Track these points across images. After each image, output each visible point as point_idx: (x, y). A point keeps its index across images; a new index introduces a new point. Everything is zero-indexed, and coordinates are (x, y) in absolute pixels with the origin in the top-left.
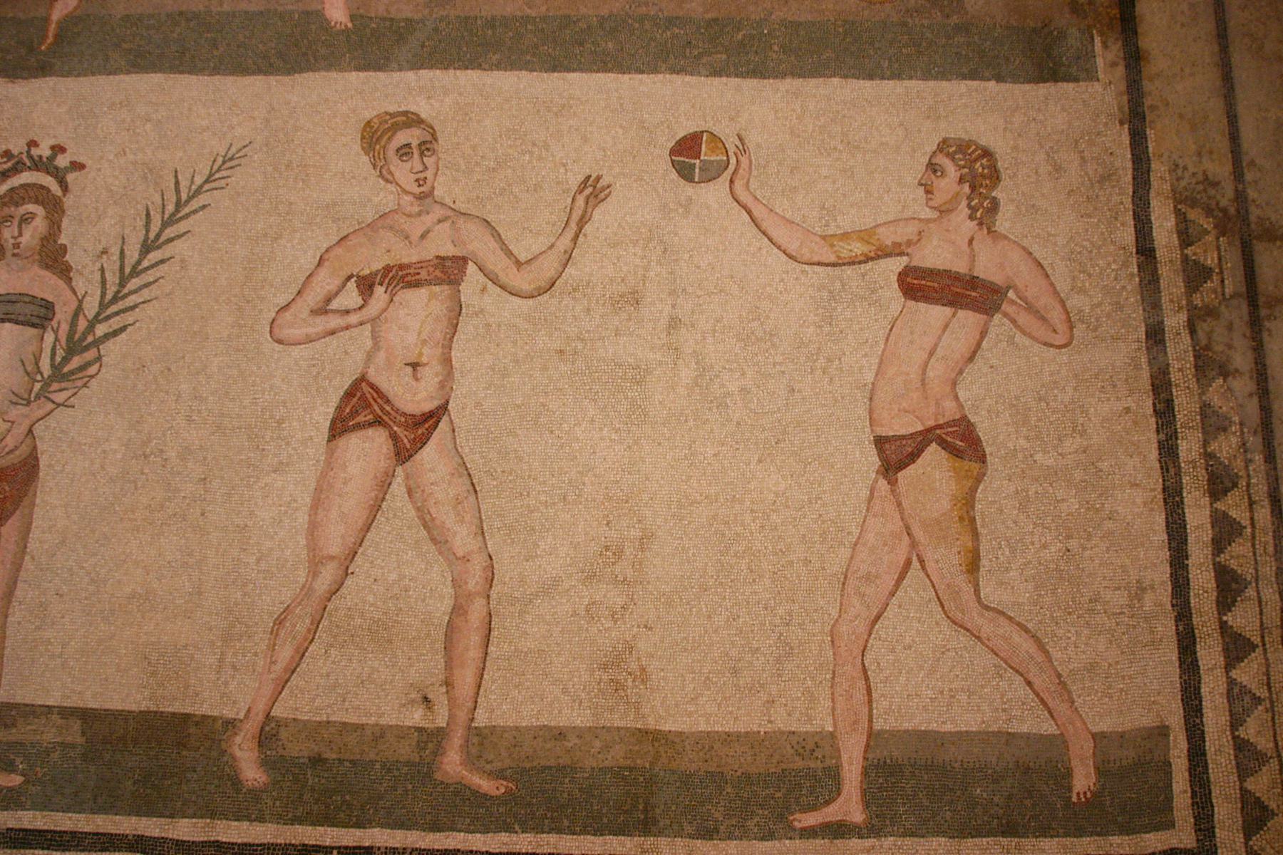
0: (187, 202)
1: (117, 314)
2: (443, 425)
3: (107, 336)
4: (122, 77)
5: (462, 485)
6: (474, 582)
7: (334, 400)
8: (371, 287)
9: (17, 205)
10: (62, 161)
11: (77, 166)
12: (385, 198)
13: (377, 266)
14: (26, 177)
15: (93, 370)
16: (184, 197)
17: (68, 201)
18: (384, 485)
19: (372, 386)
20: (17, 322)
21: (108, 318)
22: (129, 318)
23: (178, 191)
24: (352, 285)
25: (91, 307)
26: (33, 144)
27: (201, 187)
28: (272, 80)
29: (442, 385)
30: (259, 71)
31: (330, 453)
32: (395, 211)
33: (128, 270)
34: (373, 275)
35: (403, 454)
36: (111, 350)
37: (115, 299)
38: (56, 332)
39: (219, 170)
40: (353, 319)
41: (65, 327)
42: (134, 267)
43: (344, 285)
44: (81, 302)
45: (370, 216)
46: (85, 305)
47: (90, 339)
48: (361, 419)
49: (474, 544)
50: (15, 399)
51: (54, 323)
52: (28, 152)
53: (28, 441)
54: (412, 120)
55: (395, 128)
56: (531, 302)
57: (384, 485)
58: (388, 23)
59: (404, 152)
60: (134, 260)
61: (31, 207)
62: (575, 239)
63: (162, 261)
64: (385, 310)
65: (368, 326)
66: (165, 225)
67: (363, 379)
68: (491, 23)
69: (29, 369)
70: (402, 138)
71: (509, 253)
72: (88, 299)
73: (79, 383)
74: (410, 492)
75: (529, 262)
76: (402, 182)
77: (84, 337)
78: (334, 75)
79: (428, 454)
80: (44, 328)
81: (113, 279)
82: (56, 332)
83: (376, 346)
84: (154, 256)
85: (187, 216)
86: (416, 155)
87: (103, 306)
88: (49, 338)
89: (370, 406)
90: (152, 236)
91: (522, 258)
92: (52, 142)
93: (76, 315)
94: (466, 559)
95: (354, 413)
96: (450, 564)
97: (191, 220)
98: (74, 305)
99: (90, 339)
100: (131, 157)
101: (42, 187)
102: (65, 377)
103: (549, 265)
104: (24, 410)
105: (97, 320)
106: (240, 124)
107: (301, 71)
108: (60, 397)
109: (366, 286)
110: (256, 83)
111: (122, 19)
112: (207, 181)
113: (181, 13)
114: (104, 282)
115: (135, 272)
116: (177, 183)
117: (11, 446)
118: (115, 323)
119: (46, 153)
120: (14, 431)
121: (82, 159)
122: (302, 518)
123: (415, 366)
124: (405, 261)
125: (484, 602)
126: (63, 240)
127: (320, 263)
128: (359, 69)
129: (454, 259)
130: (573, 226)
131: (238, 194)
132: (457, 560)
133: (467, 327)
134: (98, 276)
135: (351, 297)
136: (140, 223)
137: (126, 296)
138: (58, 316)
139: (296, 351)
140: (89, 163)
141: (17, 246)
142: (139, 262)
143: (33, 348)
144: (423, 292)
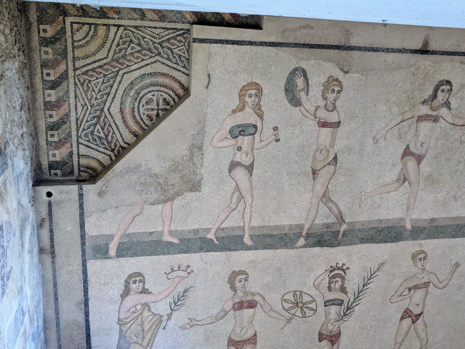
0: (373, 274)
1: (357, 301)
2: (422, 316)
3: (355, 306)
4: (359, 245)
5: (424, 326)
6: (424, 343)
7: (401, 314)
8: (411, 290)
9: (334, 279)
10: (345, 267)
11: (348, 268)
12: (415, 270)
13: (412, 285)
14: (336, 272)
15: (352, 313)
16: (372, 273)
17: (346, 277)
18: (410, 328)
19: (410, 310)
20: (335, 305)
21: (356, 302)
22: (360, 301)
23: (371, 272)
24: (407, 290)
25: (352, 300)
26: (337, 264)
27: (376, 271)
28: (393, 244)
29: (423, 308)
30: (390, 242)
31: (400, 323)
32: (417, 273)
33: (360, 291)
34: (411, 287)
35: (414, 322)
36: (356, 308)
37: (357, 298)
38: (344, 306)
39: (380, 267)
40: (407, 297)
41: (346, 305)
42: (361, 290)
43: (405, 290)
44: (349, 299)
45: (412, 275)
46: (350, 300)
47: (352, 307)
48: (406, 316)
49: (425, 337)
50: (335, 321)
51: (344, 304)
52: (336, 266)
53: (339, 329)
54: (423, 252)
55: (419, 254)
56: (441, 290)
57: (410, 328)
58: (419, 228)
59: (420, 259)
60: (361, 289)
61: (338, 279)
62: (452, 276)
63: (367, 288)
64: (413, 294)
65: (409, 298)
66: (368, 280)
67: (407, 309)
68: (442, 227)
69: (338, 314)
70: (421, 256)
71: (439, 280)
72: (351, 298)
73: (349, 316)
74: (414, 329)
75: (442, 282)
76: (419, 266)
77: (350, 307)
78: (406, 242)
79: (419, 322)
80: (341, 305)
81: (356, 294)
82: (344, 306)
83: (411, 302)
84: (366, 287)
85: (373, 278)
86: (423, 260)
87: (354, 299)
88: (343, 307)
89: (408, 314)
90: (365, 283)
91: (441, 281)
92: (342, 263)
93: (349, 302)
94: (423, 340)
95: (405, 315)
96: (420, 341)
97: (374, 279)
98: (348, 300)
99: (352, 307)
100: (361, 265)
101: (340, 274)
102: (346, 315)
103: (446, 282)
104: (338, 323)
105: (353, 302)
106: (385, 255)
107: (400, 241)
108: (345, 319)
109: (410, 290)
110: (390, 244)
111: (358, 230)
112: (377, 270)
113: (372, 228)
114: (355, 294)
115: (361, 291)
116: (371, 270)
117: (335, 330)
118: (357, 303)
119: (341, 266)
120: (336, 327)
121: (349, 267)
122: (394, 336)
123: (418, 305)
124: (418, 284)
125: (425, 346)
126: (345, 286)
127: (401, 286)
128: (412, 240)
129: (428, 282)
130: (452, 273)
131: (384, 272)
132: (421, 340)
133: (429, 296)
134: (353, 293)
135: (406, 292)
136: (363, 280)
137: (359, 297)
138: (344, 303)
139: (394, 305)
140: (351, 267)
141: (335, 288)
142: (362, 289)
143: (339, 310)
144: (421, 290)
